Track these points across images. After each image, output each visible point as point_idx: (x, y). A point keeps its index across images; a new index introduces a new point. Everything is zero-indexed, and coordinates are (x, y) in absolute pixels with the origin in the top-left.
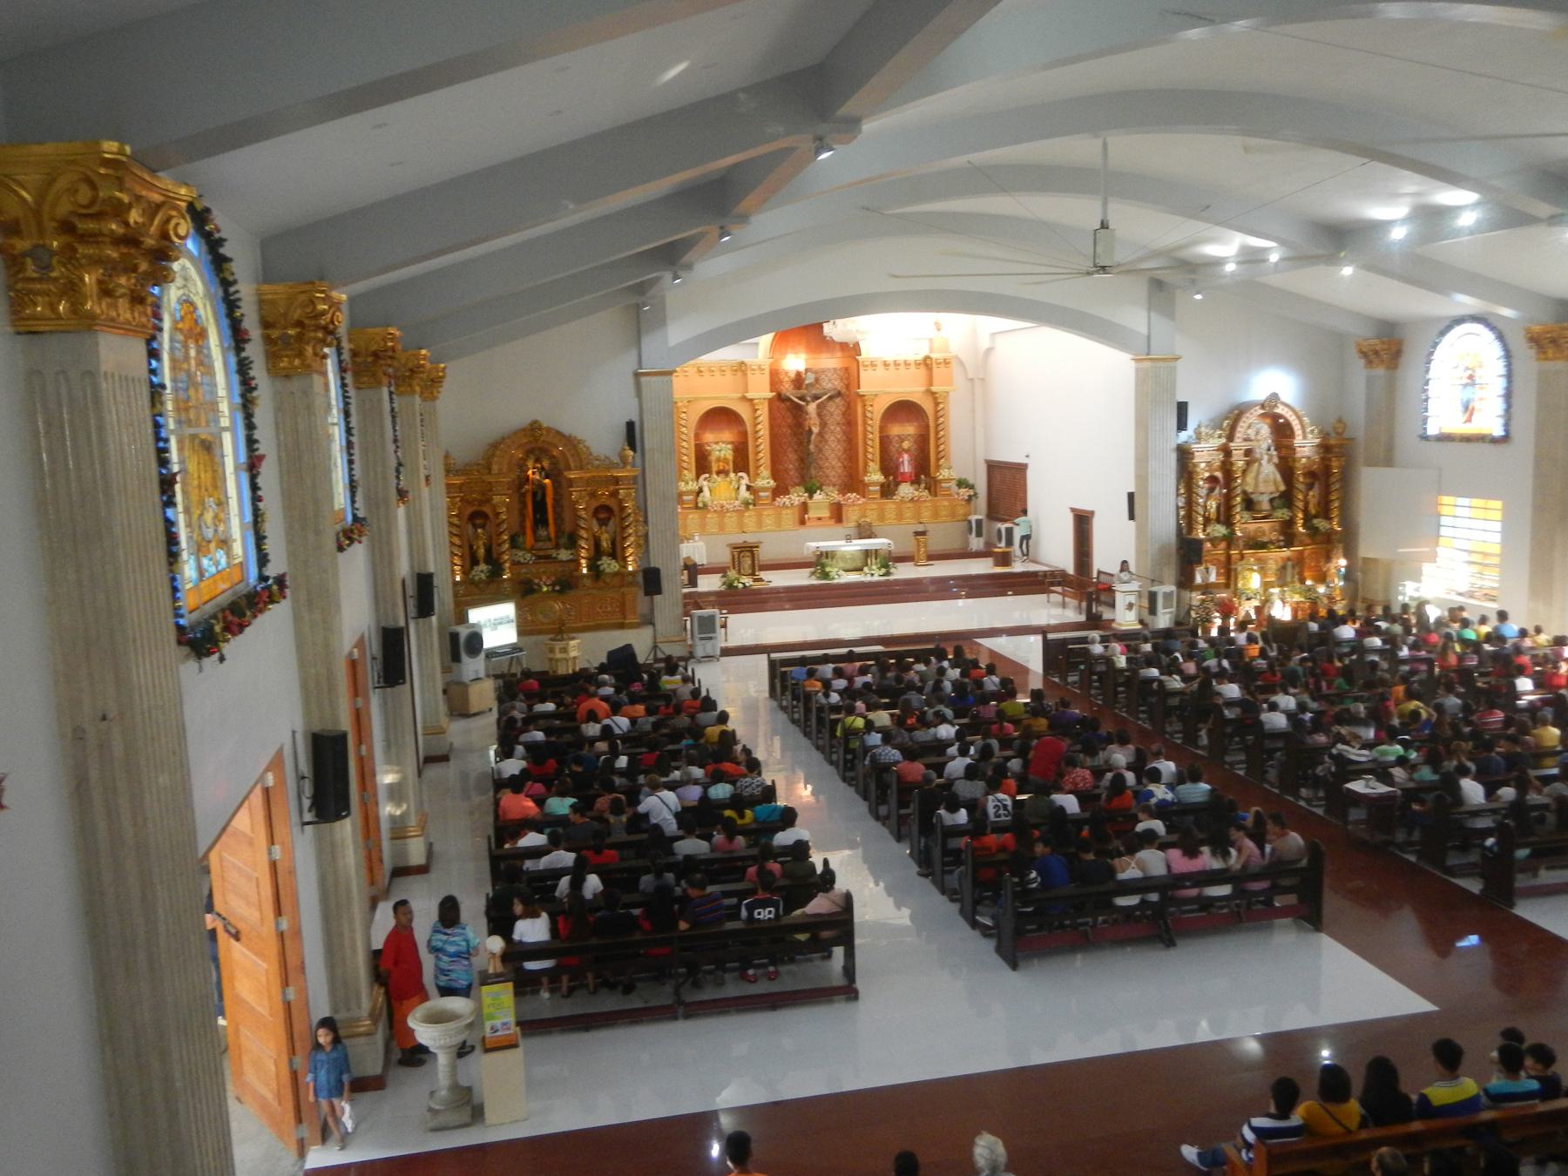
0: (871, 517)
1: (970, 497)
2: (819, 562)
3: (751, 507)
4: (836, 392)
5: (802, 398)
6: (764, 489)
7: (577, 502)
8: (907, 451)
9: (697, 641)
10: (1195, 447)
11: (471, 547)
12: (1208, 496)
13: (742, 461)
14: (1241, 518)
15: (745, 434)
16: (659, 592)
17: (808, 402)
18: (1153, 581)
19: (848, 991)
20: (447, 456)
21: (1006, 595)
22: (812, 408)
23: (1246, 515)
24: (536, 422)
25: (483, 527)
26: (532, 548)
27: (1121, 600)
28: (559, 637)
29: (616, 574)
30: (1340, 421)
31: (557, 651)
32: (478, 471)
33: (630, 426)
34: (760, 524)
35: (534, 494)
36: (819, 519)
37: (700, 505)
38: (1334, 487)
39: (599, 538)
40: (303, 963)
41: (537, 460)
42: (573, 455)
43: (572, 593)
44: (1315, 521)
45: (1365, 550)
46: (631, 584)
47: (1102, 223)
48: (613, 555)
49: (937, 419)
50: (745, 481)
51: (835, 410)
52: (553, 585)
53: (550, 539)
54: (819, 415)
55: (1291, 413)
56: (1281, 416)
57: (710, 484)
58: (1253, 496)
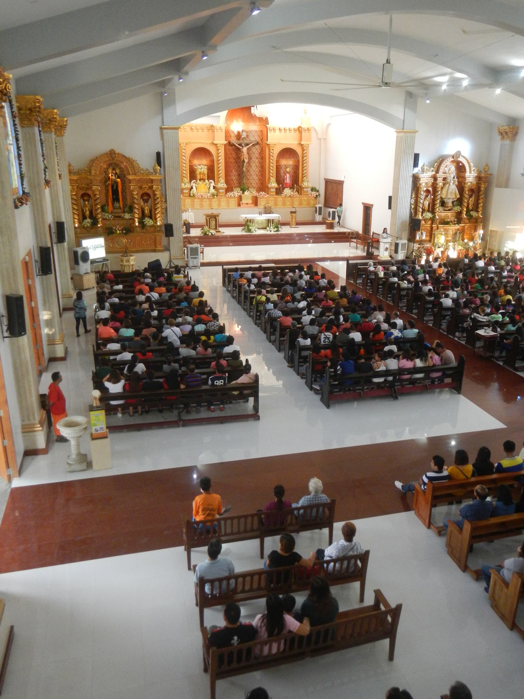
0: (271, 204)
2: (246, 224)
3: (215, 197)
5: (240, 145)
6: (222, 189)
7: (133, 191)
8: (289, 173)
9: (189, 259)
10: (421, 176)
11: (83, 211)
13: (211, 175)
14: (438, 209)
16: (172, 235)
17: (243, 147)
18: (397, 238)
19: (255, 416)
20: (69, 165)
21: (331, 242)
22: (245, 149)
24: (112, 150)
25: (88, 201)
26: (112, 212)
27: (382, 246)
28: (126, 255)
29: (152, 226)
30: (487, 165)
31: (125, 262)
32: (85, 174)
33: (158, 154)
34: (219, 205)
35: (113, 186)
36: (247, 204)
37: (192, 195)
38: (481, 197)
39: (144, 208)
40: (6, 400)
41: (114, 169)
42: (131, 168)
43: (131, 234)
44: (471, 212)
45: (492, 227)
46: (159, 231)
47: (387, 60)
48: (150, 217)
49: (303, 157)
50: (213, 184)
51: (256, 151)
52: (122, 230)
53: (120, 208)
54: (248, 153)
55: (465, 161)
56: (461, 162)
58: (445, 200)
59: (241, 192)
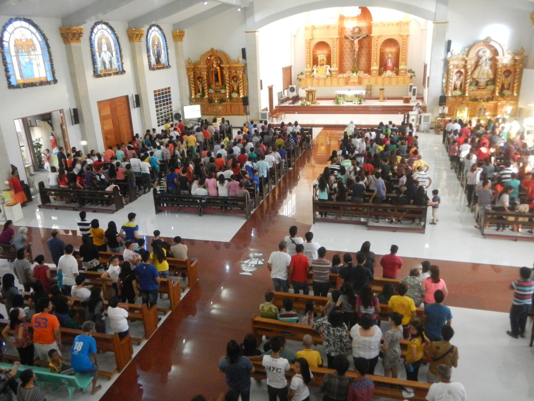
0: (373, 82)
1: (411, 77)
2: (336, 99)
4: (366, 35)
5: (353, 38)
6: (333, 71)
12: (457, 79)
13: (329, 62)
15: (330, 51)
17: (355, 39)
20: (189, 59)
23: (473, 87)
29: (237, 98)
30: (522, 48)
33: (244, 51)
34: (331, 84)
35: (215, 71)
36: (354, 83)
45: (520, 105)
57: (317, 69)
58: (477, 80)
59: (352, 74)
